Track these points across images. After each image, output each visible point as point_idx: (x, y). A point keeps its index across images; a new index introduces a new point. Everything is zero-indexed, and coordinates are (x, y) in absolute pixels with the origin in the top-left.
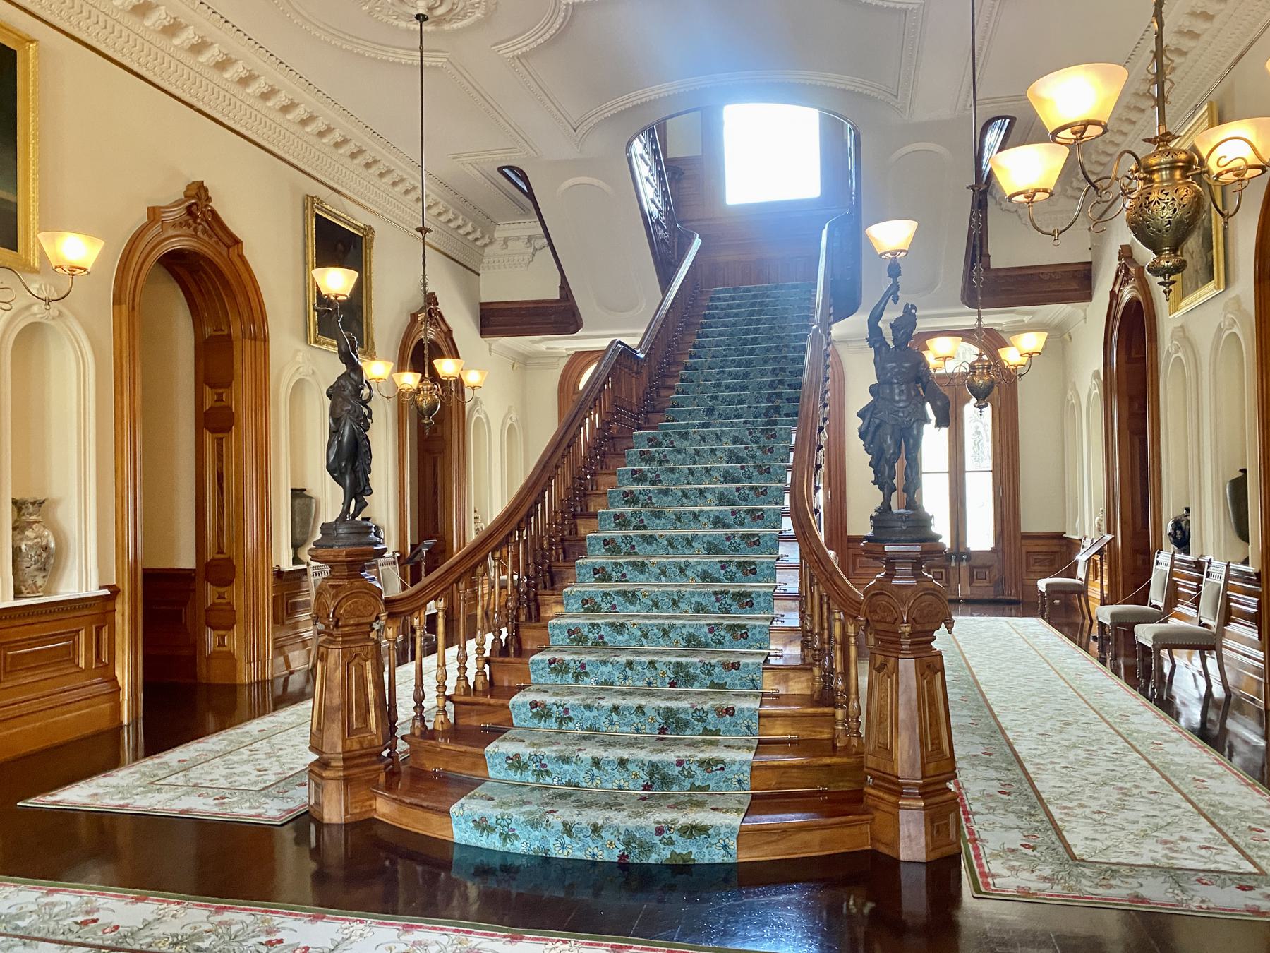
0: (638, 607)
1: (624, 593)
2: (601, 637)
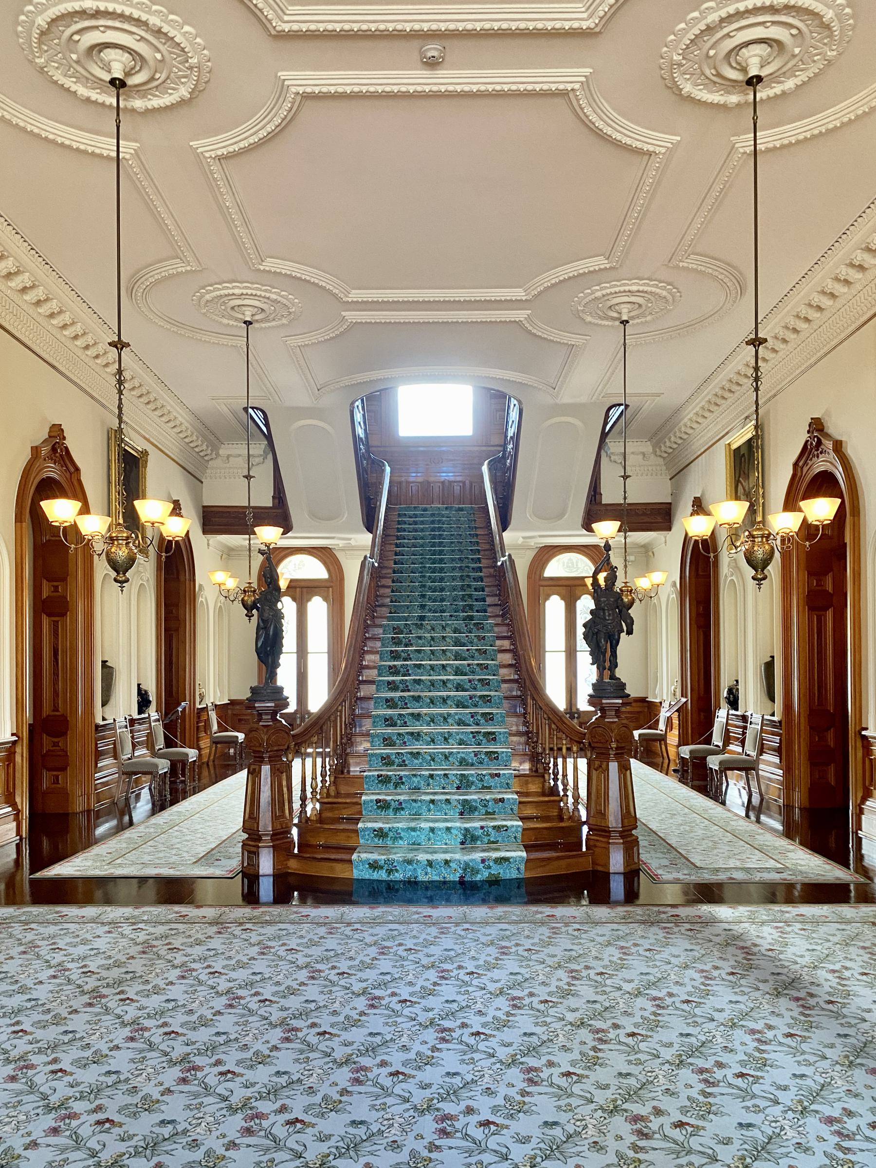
0: (421, 742)
1: (412, 734)
2: (404, 761)
